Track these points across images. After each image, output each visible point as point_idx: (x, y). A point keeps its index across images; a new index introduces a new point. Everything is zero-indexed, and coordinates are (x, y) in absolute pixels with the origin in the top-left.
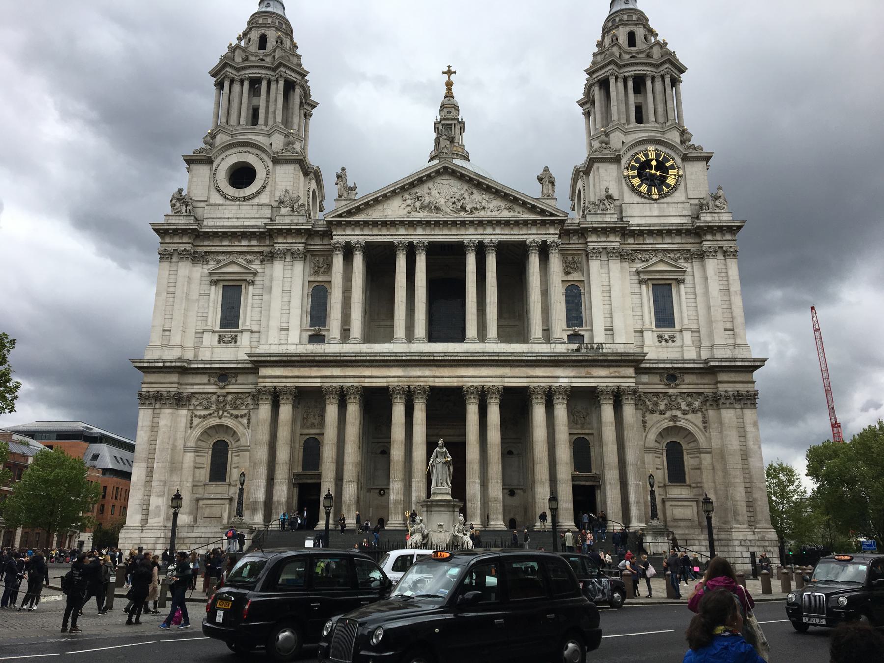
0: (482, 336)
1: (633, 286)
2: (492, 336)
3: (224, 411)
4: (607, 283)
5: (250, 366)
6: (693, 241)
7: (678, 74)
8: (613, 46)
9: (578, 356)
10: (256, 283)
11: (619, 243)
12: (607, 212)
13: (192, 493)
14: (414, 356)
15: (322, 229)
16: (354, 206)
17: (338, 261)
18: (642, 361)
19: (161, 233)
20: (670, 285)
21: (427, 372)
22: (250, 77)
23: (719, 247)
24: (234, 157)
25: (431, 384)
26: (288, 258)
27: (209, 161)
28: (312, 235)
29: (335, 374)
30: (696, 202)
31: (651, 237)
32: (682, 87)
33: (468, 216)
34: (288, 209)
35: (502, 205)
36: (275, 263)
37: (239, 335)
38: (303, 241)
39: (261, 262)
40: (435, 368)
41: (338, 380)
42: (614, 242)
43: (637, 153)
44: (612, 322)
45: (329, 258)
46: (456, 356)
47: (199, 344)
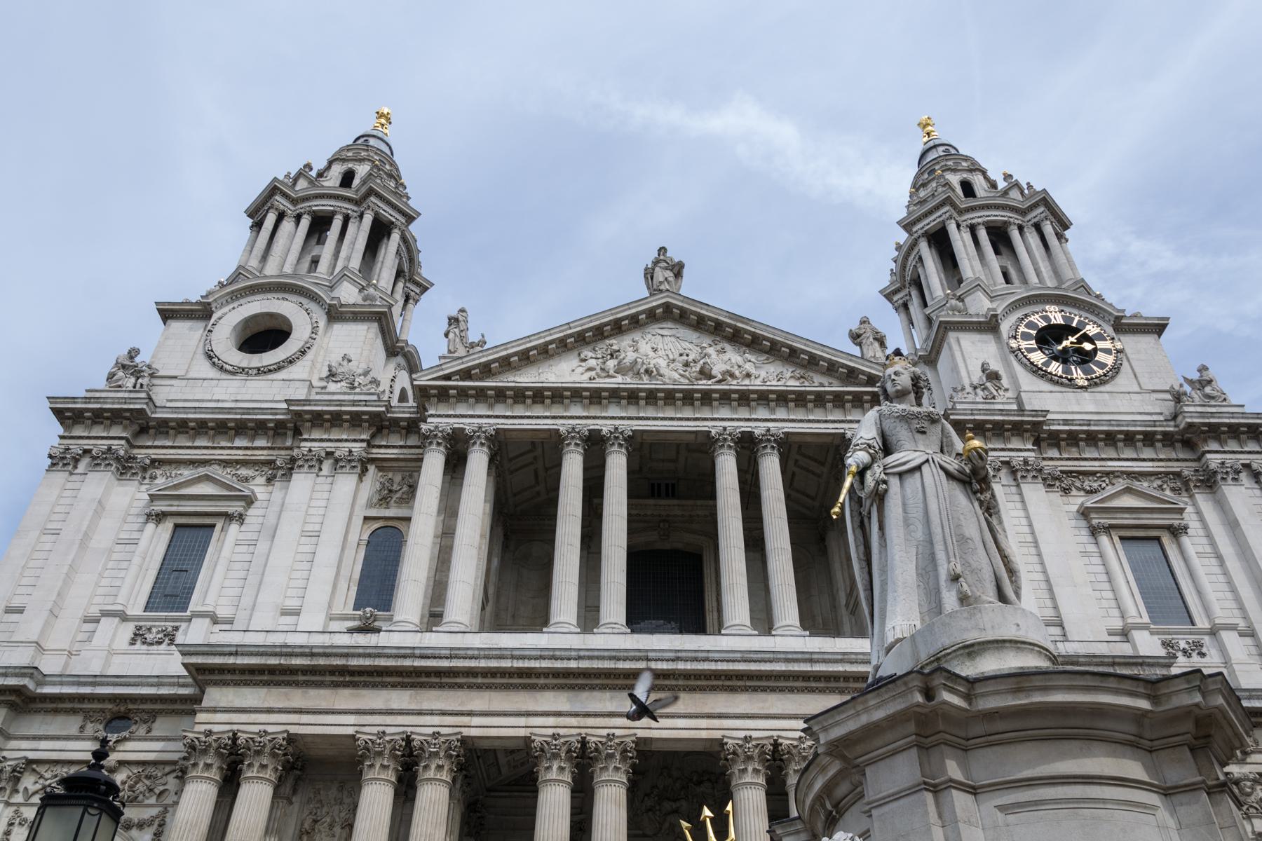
4: (1026, 529)
6: (1181, 456)
11: (1033, 454)
14: (598, 658)
15: (408, 415)
17: (434, 463)
19: (69, 418)
20: (1158, 539)
22: (314, 211)
23: (1243, 465)
26: (327, 466)
29: (395, 705)
31: (1093, 449)
32: (1070, 246)
34: (343, 383)
35: (785, 371)
36: (295, 476)
37: (183, 625)
39: (270, 480)
42: (1021, 451)
44: (1056, 607)
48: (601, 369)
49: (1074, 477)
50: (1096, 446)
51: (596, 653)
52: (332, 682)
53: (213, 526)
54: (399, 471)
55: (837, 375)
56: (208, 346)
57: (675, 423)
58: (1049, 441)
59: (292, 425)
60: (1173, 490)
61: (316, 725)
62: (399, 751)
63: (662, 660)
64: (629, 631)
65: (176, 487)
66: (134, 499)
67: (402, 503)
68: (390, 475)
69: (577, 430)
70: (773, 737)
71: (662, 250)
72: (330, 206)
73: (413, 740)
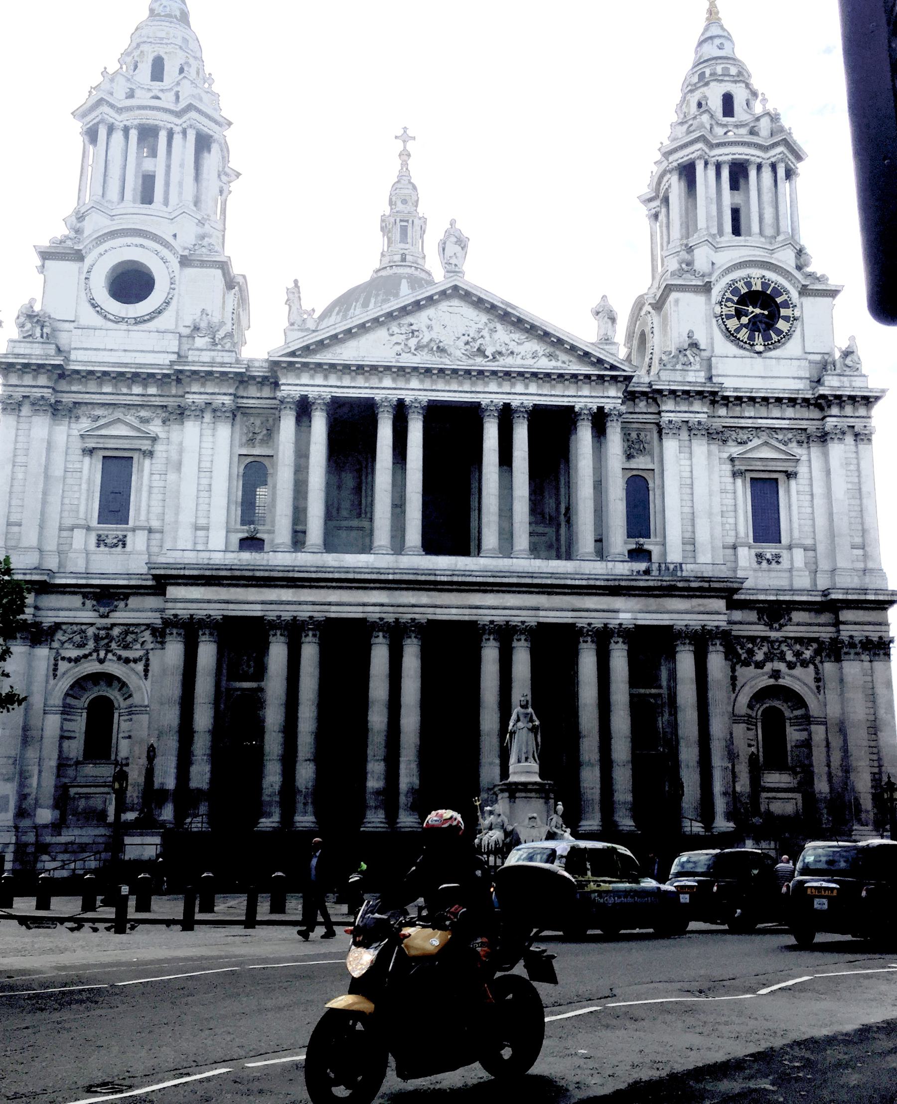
0: (506, 547)
1: (723, 480)
2: (522, 548)
3: (107, 652)
4: (688, 474)
5: (150, 583)
6: (811, 417)
7: (793, 160)
8: (700, 115)
9: (648, 580)
10: (157, 454)
11: (706, 416)
12: (689, 368)
13: (58, 776)
16: (314, 340)
17: (288, 425)
18: (736, 590)
20: (776, 480)
21: (423, 598)
23: (849, 426)
25: (431, 617)
26: (208, 417)
27: (79, 257)
28: (246, 382)
29: (284, 599)
30: (818, 358)
31: (752, 408)
32: (800, 181)
33: (488, 363)
34: (207, 339)
38: (231, 391)
39: (164, 422)
41: (288, 607)
42: (699, 412)
43: (734, 281)
44: (694, 532)
45: (271, 420)
46: (470, 576)
47: (66, 548)
48: (406, 345)
50: (754, 406)
57: (457, 395)
59: (174, 378)
60: (798, 442)
65: (98, 428)
66: (69, 436)
71: (453, 223)
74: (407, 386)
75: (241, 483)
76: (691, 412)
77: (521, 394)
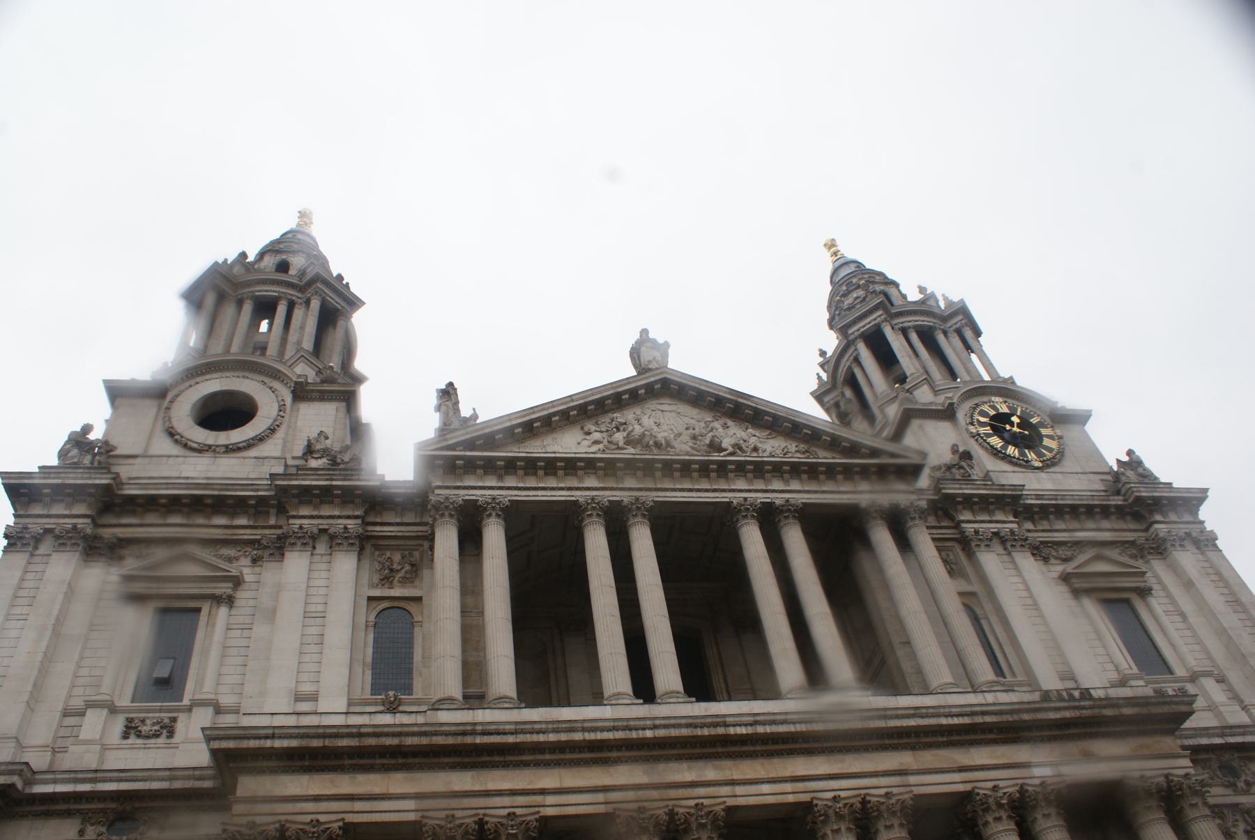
4: (1025, 594)
5: (208, 784)
10: (238, 602)
11: (1014, 526)
14: (674, 726)
16: (482, 432)
20: (1127, 601)
21: (709, 772)
24: (213, 385)
25: (731, 802)
26: (321, 548)
31: (1060, 522)
34: (324, 460)
36: (288, 555)
37: (182, 717)
38: (357, 513)
40: (728, 763)
41: (467, 802)
42: (1006, 523)
44: (1066, 662)
45: (416, 554)
48: (609, 442)
49: (1049, 547)
51: (672, 722)
52: (383, 765)
53: (198, 610)
54: (397, 550)
55: (840, 449)
56: (168, 423)
57: (694, 494)
58: (1025, 515)
61: (372, 812)
62: (472, 835)
63: (740, 725)
64: (694, 699)
67: (406, 583)
68: (388, 554)
69: (596, 501)
70: (860, 795)
71: (644, 332)
72: (274, 291)
73: (487, 822)
74: (620, 486)
75: (371, 637)
76: (997, 522)
77: (783, 491)
